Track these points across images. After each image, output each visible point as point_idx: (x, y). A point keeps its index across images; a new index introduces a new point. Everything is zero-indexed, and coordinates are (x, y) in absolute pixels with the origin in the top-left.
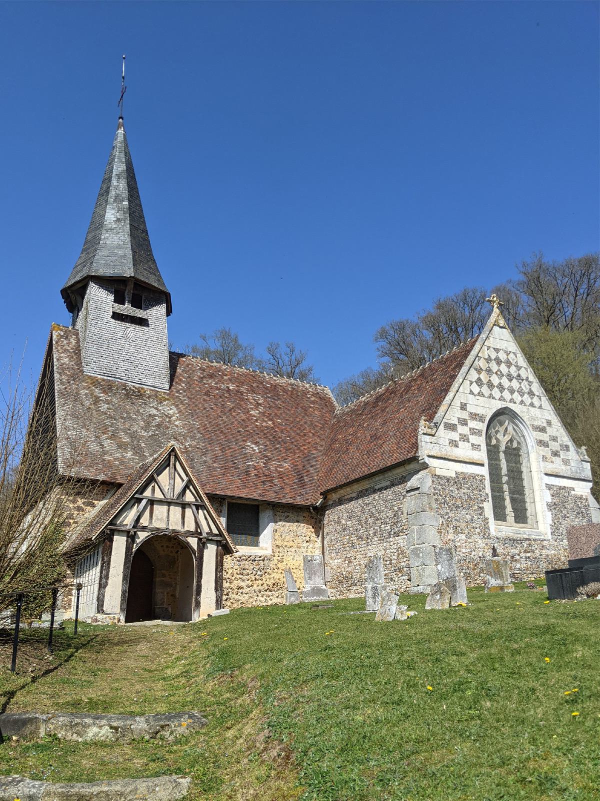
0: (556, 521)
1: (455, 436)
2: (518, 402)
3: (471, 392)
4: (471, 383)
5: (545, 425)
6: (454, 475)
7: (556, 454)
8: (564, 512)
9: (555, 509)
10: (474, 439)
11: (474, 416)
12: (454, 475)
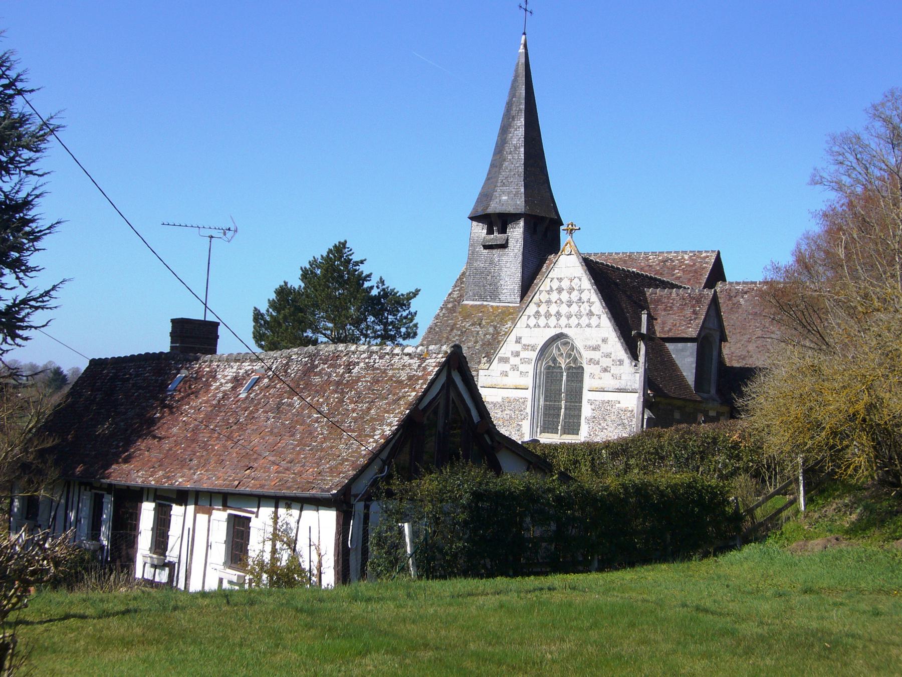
0: (592, 433)
1: (506, 367)
2: (573, 326)
3: (528, 326)
4: (529, 317)
5: (600, 343)
6: (500, 400)
7: (605, 370)
8: (602, 424)
9: (593, 422)
10: (523, 368)
11: (526, 347)
12: (500, 400)
